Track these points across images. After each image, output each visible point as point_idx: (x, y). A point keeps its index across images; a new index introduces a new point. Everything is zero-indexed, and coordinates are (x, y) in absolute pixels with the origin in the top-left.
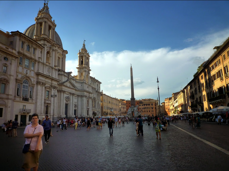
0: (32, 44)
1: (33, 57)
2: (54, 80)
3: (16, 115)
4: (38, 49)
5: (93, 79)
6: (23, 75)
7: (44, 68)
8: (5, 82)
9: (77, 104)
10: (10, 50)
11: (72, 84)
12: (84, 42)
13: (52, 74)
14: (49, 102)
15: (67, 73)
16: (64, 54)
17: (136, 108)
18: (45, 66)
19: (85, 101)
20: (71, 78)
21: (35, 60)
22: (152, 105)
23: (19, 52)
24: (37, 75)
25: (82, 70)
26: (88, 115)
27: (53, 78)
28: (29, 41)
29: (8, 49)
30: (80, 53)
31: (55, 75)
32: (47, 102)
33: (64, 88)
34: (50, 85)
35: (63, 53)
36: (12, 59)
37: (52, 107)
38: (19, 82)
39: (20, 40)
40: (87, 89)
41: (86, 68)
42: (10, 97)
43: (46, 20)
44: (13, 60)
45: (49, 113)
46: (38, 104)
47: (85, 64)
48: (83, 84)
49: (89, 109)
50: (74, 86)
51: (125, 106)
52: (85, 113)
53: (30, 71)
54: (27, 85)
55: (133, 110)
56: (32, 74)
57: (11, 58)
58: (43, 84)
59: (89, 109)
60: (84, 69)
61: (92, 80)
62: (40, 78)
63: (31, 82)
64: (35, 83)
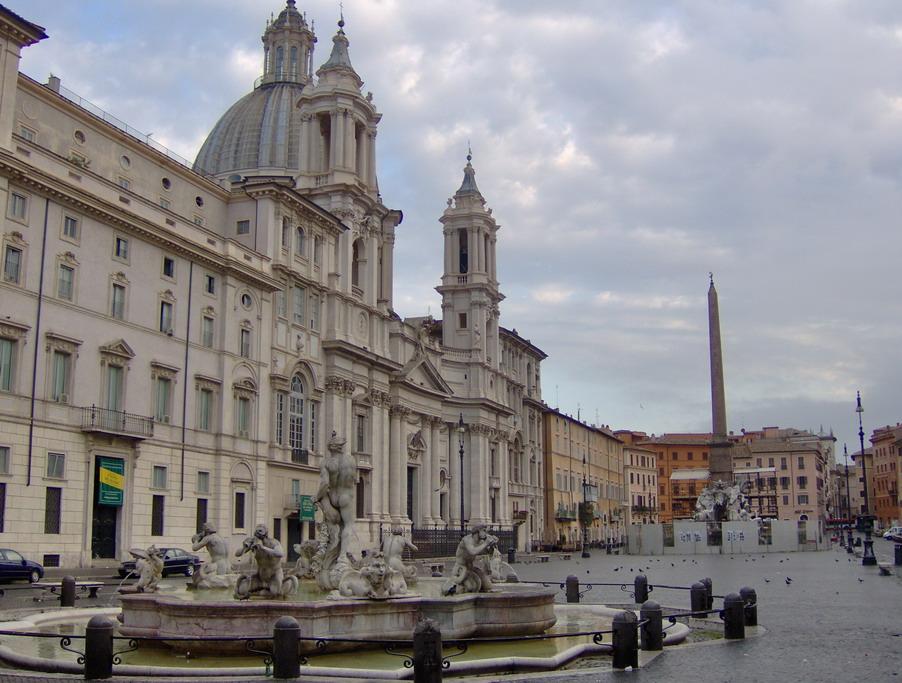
1: (314, 277)
3: (275, 519)
4: (326, 236)
9: (447, 467)
10: (255, 263)
12: (469, 158)
13: (371, 337)
15: (407, 323)
16: (386, 230)
17: (734, 493)
19: (481, 450)
21: (322, 290)
23: (276, 268)
25: (462, 303)
26: (494, 521)
27: (378, 357)
29: (248, 258)
33: (407, 399)
35: (385, 224)
36: (262, 299)
38: (278, 387)
39: (277, 214)
40: (491, 395)
42: (263, 450)
45: (365, 512)
48: (473, 369)
49: (497, 490)
53: (309, 339)
55: (720, 501)
58: (347, 387)
59: (497, 490)
60: (476, 296)
61: (505, 347)
62: (341, 363)
64: (321, 386)
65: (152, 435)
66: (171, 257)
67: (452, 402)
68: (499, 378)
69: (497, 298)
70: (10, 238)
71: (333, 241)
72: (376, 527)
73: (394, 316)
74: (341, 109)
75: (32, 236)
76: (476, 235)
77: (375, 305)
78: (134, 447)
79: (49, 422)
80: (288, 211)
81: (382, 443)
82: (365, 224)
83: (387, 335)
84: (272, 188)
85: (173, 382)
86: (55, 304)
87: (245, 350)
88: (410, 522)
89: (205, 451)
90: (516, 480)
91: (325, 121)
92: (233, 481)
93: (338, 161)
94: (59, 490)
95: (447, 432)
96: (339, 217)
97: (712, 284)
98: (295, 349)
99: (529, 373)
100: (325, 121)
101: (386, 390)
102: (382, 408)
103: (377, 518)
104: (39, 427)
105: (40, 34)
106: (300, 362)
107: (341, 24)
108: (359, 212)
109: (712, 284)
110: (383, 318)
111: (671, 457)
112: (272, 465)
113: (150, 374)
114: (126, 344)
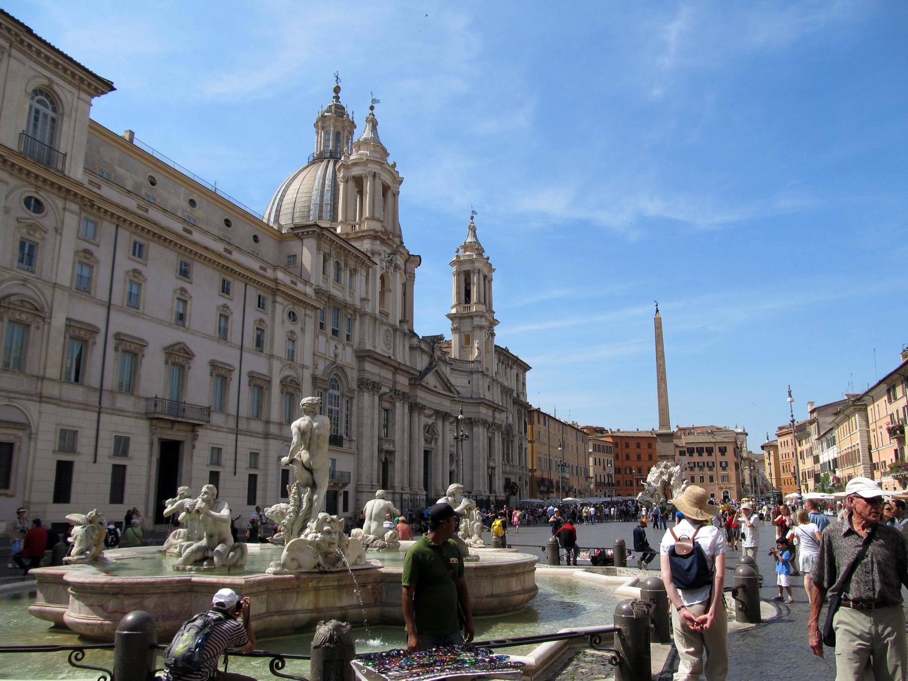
0: (346, 256)
2: (401, 370)
4: (359, 269)
5: (503, 354)
6: (328, 362)
7: (377, 332)
8: (292, 389)
9: (455, 450)
10: (300, 286)
11: (442, 379)
14: (391, 448)
16: (408, 270)
18: (377, 326)
19: (481, 438)
20: (439, 359)
21: (355, 310)
22: (723, 451)
23: (318, 291)
25: (467, 326)
26: (491, 492)
27: (400, 363)
28: (338, 250)
29: (295, 284)
30: (458, 262)
31: (401, 354)
32: (386, 447)
33: (422, 397)
34: (391, 391)
35: (408, 265)
37: (397, 464)
38: (319, 385)
41: (482, 316)
43: (376, 168)
44: (307, 319)
46: (365, 454)
47: (479, 302)
49: (493, 468)
50: (447, 387)
51: (610, 458)
52: (484, 483)
53: (344, 349)
54: (337, 393)
55: (665, 477)
56: (347, 357)
57: (302, 311)
59: (493, 468)
60: (477, 321)
61: (499, 360)
62: (369, 366)
63: (348, 384)
64: (354, 385)
65: (208, 422)
66: (228, 278)
67: (459, 401)
68: (495, 383)
69: (494, 323)
70: (82, 254)
71: (364, 273)
72: (397, 497)
73: (413, 335)
74: (371, 172)
75: (103, 253)
76: (476, 275)
77: (398, 324)
78: (193, 431)
79: (116, 410)
80: (328, 247)
81: (403, 431)
82: (391, 262)
83: (407, 347)
84: (314, 229)
85: (228, 379)
86: (123, 312)
87: (291, 355)
88: (425, 493)
89: (256, 435)
90: (508, 462)
91: (359, 182)
93: (367, 214)
94: (124, 467)
95: (455, 424)
96: (369, 255)
97: (657, 311)
98: (333, 356)
99: (517, 380)
100: (359, 182)
101: (407, 390)
102: (403, 403)
103: (398, 490)
104: (107, 413)
105: (109, 87)
106: (337, 367)
107: (372, 108)
108: (385, 252)
109: (657, 311)
110: (405, 334)
111: (624, 446)
113: (209, 371)
114: (187, 347)
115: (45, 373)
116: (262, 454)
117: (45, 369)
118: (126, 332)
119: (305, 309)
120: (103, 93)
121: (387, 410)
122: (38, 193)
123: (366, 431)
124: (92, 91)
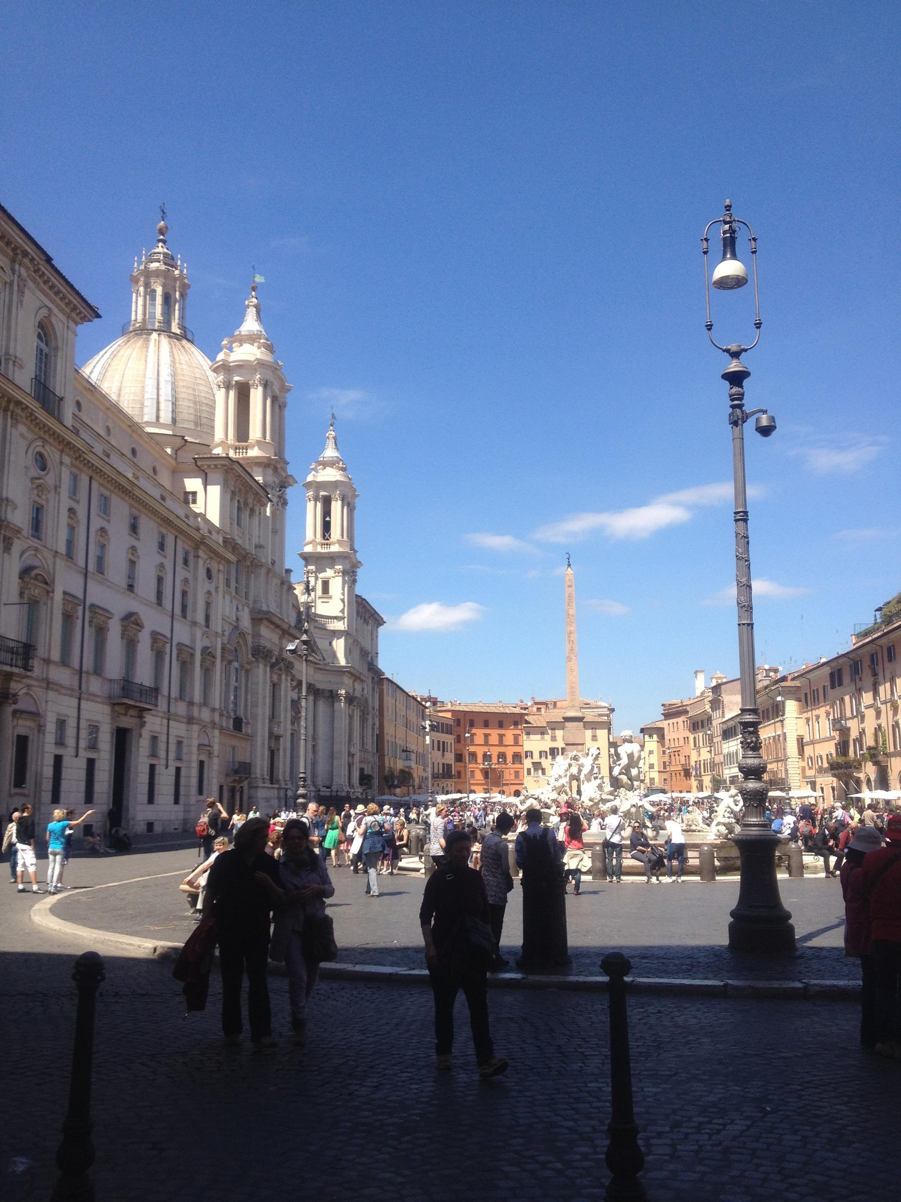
24: (253, 619)
43: (270, 376)
52: (345, 775)
55: (574, 770)
65: (156, 706)
72: (282, 793)
78: (141, 717)
92: (199, 745)
93: (255, 432)
98: (234, 619)
112: (221, 729)
115: (49, 655)
116: (185, 741)
117: (49, 651)
118: (102, 605)
119: (219, 563)
120: (90, 321)
121: (274, 685)
122: (43, 447)
123: (260, 710)
124: (78, 319)
